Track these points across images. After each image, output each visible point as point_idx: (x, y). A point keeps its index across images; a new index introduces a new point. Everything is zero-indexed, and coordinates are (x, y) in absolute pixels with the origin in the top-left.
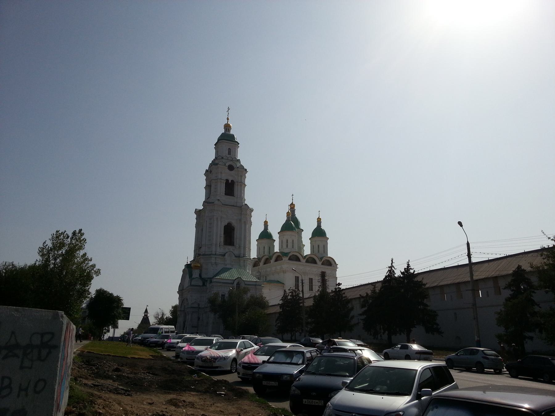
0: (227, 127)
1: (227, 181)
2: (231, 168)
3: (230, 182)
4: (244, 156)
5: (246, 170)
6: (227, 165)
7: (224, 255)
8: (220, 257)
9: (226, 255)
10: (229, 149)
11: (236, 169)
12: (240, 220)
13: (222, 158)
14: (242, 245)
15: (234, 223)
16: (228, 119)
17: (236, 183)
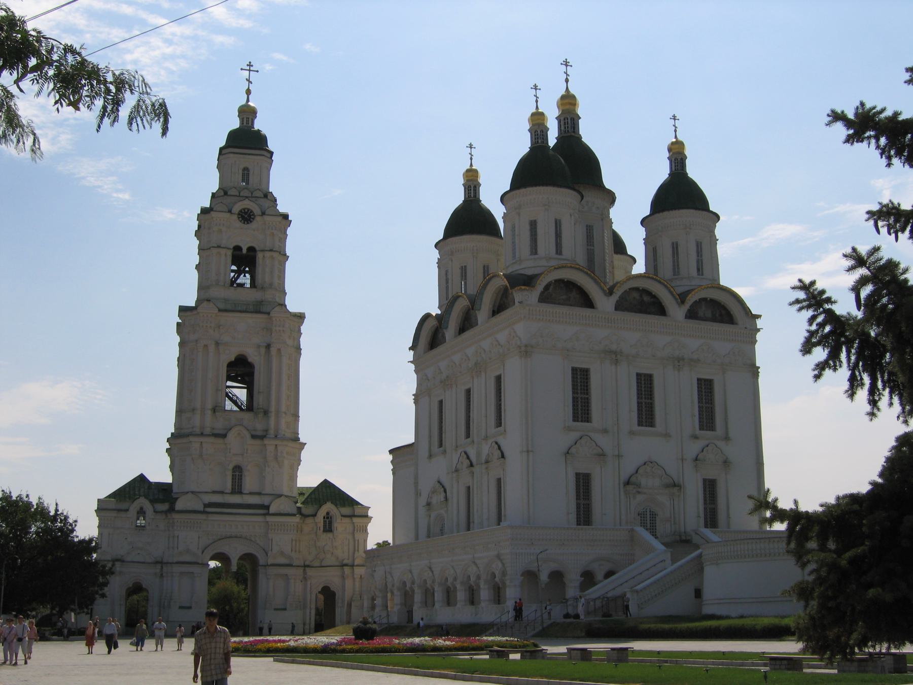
0: (247, 113)
1: (237, 248)
2: (246, 217)
3: (244, 251)
4: (285, 184)
5: (285, 217)
6: (237, 209)
7: (224, 436)
8: (212, 439)
9: (231, 436)
10: (246, 170)
11: (258, 219)
12: (268, 347)
13: (226, 193)
14: (273, 409)
15: (254, 357)
16: (248, 92)
17: (260, 255)
